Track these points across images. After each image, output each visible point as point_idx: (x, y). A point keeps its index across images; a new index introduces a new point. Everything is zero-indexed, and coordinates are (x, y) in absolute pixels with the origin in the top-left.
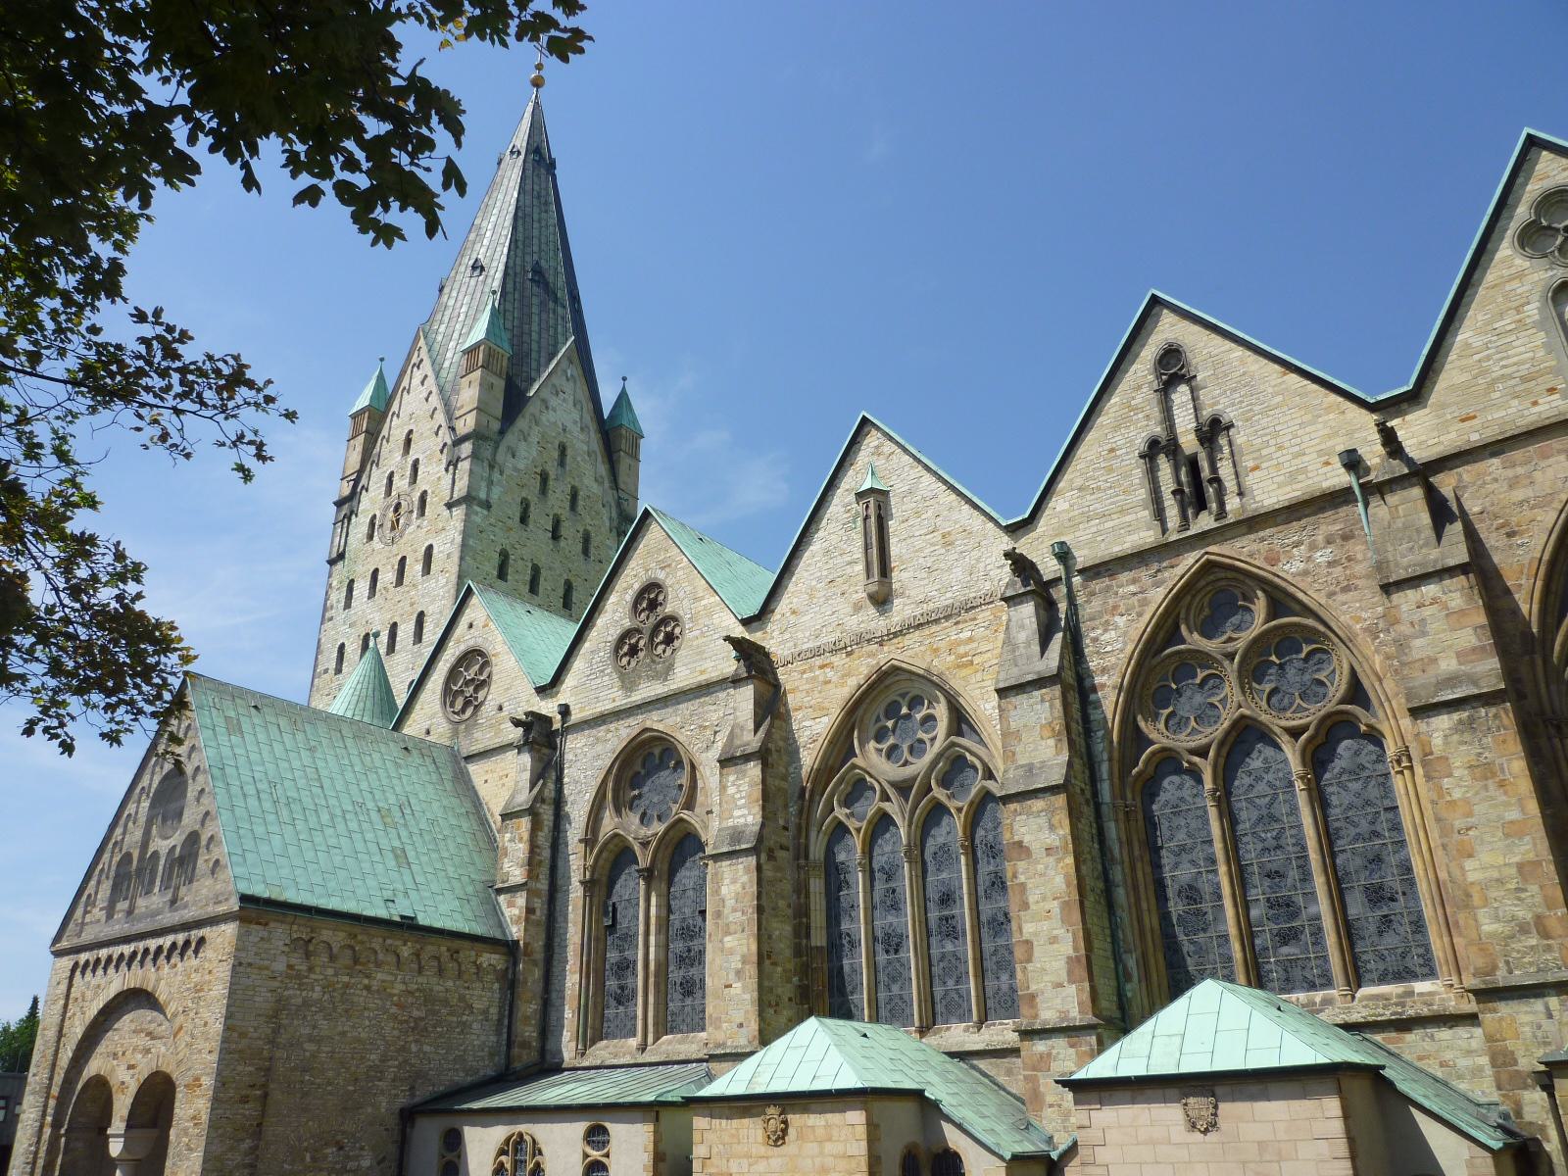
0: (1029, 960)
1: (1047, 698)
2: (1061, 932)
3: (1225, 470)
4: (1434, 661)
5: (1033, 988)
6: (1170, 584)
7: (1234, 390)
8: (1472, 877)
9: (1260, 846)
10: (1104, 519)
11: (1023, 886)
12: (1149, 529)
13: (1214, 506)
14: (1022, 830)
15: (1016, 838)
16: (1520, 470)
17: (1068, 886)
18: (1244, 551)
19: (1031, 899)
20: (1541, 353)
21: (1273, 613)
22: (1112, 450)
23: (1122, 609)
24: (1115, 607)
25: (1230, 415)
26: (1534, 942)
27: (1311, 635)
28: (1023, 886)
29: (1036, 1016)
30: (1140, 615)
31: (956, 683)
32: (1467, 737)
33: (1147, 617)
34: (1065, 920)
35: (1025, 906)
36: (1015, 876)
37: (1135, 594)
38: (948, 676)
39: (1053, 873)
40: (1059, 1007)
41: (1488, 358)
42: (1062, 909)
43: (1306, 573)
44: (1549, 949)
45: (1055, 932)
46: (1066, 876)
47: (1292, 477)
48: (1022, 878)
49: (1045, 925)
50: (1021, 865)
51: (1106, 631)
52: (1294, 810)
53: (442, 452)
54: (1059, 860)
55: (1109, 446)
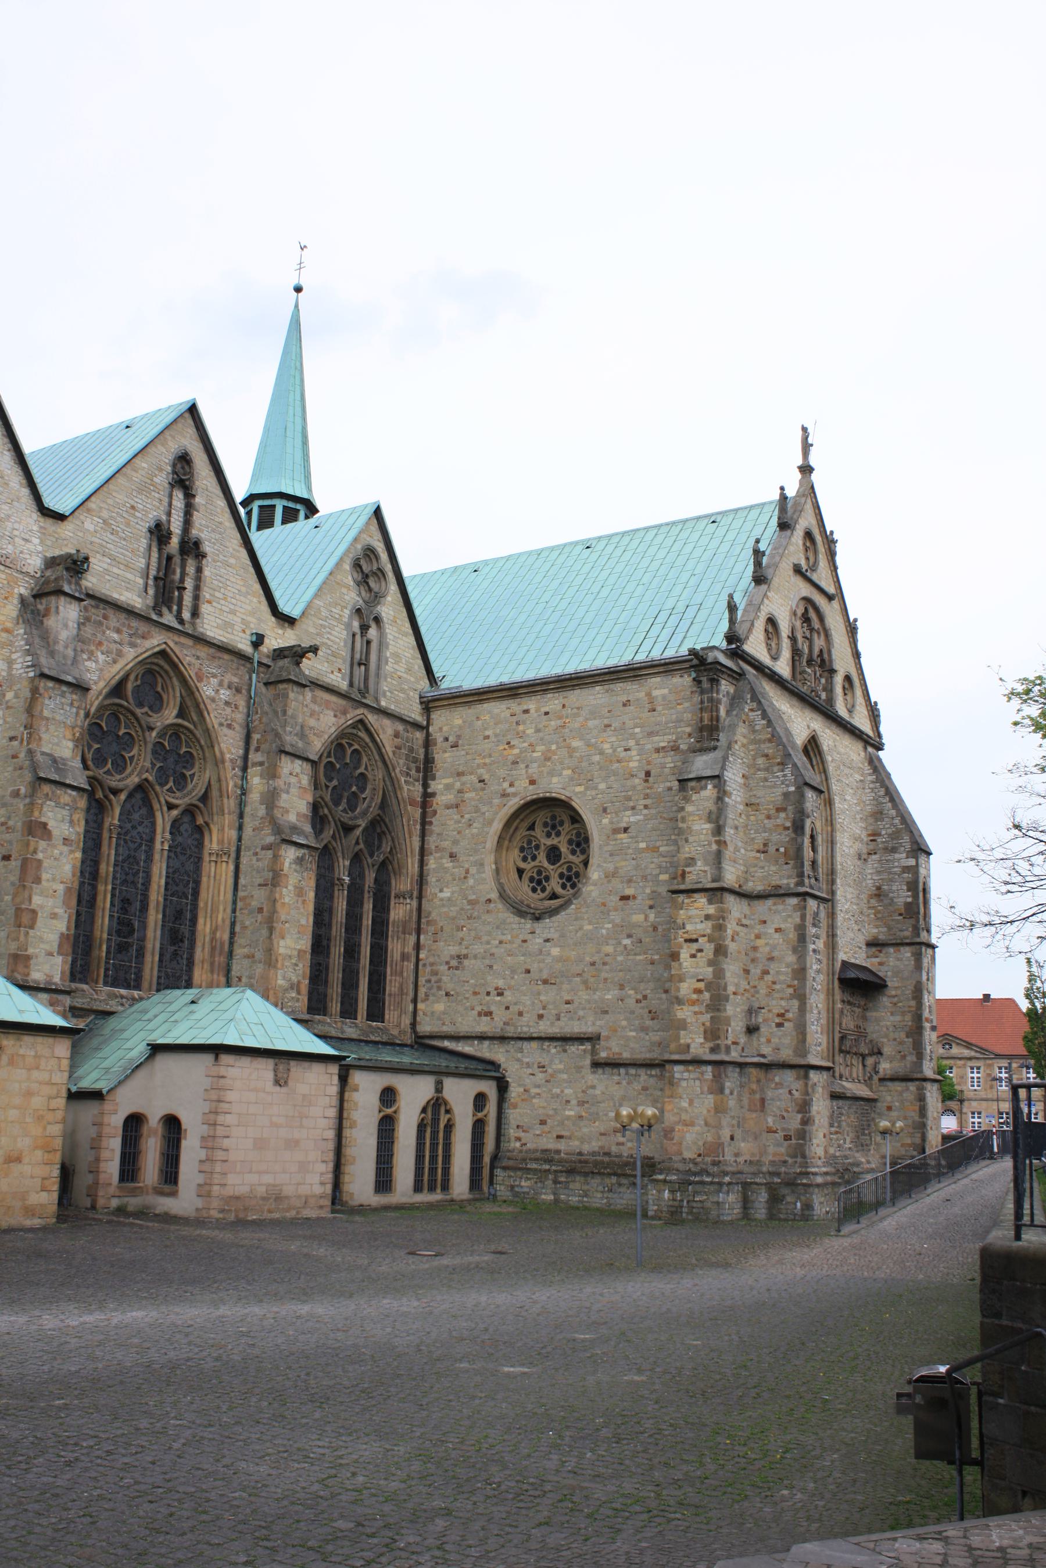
0: (32, 927)
1: (76, 704)
2: (60, 911)
3: (189, 584)
4: (287, 812)
5: (31, 951)
6: (140, 650)
7: (213, 531)
8: (282, 951)
9: (124, 877)
10: (114, 563)
11: (40, 862)
12: (139, 596)
13: (175, 608)
14: (50, 814)
15: (43, 819)
16: (317, 708)
17: (74, 876)
18: (188, 656)
19: (45, 876)
20: (342, 644)
21: (182, 713)
22: (133, 507)
23: (104, 648)
24: (100, 644)
25: (207, 547)
26: (294, 995)
28: (40, 862)
29: (28, 975)
30: (115, 662)
32: (298, 868)
33: (118, 667)
35: (38, 880)
36: (35, 852)
37: (115, 642)
39: (65, 861)
40: (47, 972)
41: (324, 627)
42: (65, 894)
43: (213, 700)
44: (298, 1000)
45: (56, 910)
46: (74, 867)
47: (227, 625)
48: (40, 856)
49: (50, 902)
50: (42, 844)
51: (89, 659)
52: (149, 859)
54: (71, 852)
55: (132, 502)
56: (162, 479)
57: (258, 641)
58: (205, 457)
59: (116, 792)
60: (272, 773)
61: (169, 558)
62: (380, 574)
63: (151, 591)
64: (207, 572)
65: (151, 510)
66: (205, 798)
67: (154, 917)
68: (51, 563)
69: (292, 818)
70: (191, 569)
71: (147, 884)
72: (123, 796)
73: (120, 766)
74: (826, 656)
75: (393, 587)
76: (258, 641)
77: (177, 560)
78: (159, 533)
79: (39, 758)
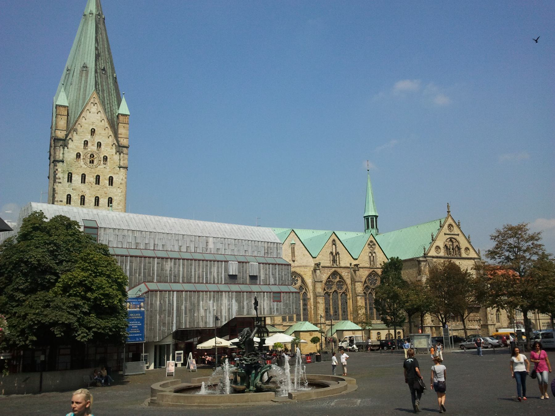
3: (338, 259)
18: (339, 270)
25: (340, 253)
27: (342, 282)
31: (304, 276)
34: (323, 312)
38: (303, 275)
47: (345, 263)
52: (338, 301)
53: (112, 146)
56: (331, 245)
57: (351, 264)
58: (337, 239)
59: (331, 293)
60: (355, 285)
61: (334, 256)
62: (374, 244)
63: (332, 262)
64: (340, 256)
65: (330, 250)
66: (346, 290)
67: (340, 310)
68: (315, 264)
69: (359, 291)
70: (338, 256)
71: (338, 305)
72: (332, 293)
73: (331, 288)
74: (459, 246)
75: (377, 245)
76: (351, 264)
77: (335, 256)
78: (332, 253)
79: (317, 293)
